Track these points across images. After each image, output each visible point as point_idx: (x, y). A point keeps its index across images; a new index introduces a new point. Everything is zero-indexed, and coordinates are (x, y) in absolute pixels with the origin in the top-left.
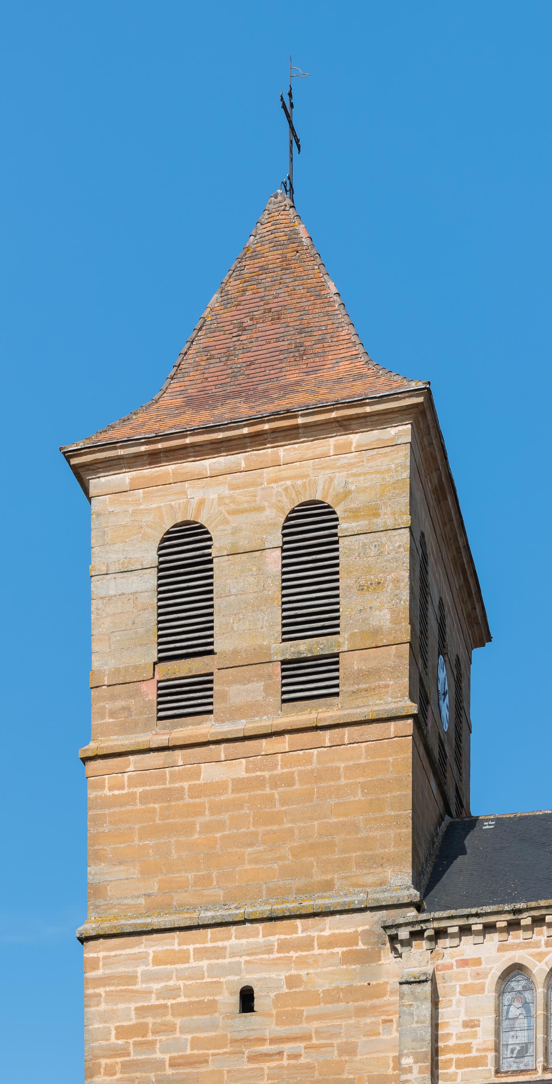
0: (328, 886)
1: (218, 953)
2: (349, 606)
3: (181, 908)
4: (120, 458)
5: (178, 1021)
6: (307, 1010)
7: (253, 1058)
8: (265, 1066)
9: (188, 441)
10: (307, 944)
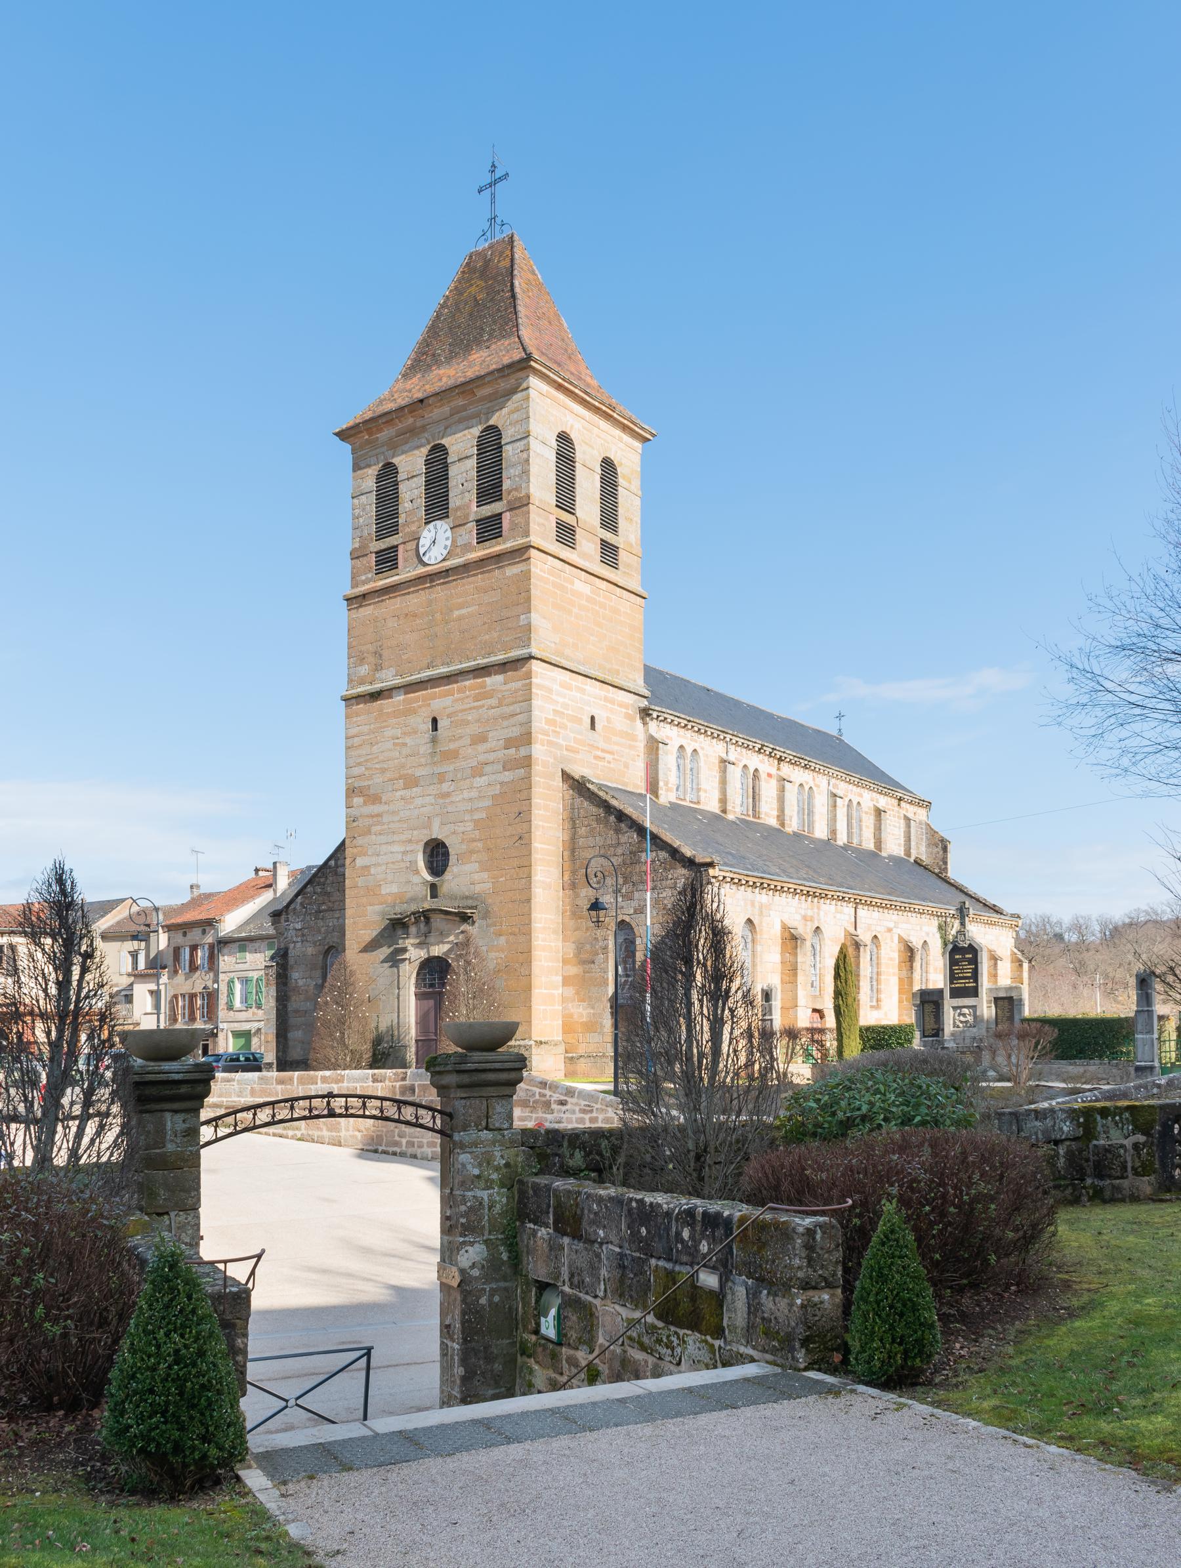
0: (618, 672)
1: (583, 691)
2: (622, 523)
3: (567, 658)
4: (548, 377)
5: (569, 724)
6: (614, 739)
7: (596, 757)
8: (601, 763)
9: (577, 391)
10: (612, 702)
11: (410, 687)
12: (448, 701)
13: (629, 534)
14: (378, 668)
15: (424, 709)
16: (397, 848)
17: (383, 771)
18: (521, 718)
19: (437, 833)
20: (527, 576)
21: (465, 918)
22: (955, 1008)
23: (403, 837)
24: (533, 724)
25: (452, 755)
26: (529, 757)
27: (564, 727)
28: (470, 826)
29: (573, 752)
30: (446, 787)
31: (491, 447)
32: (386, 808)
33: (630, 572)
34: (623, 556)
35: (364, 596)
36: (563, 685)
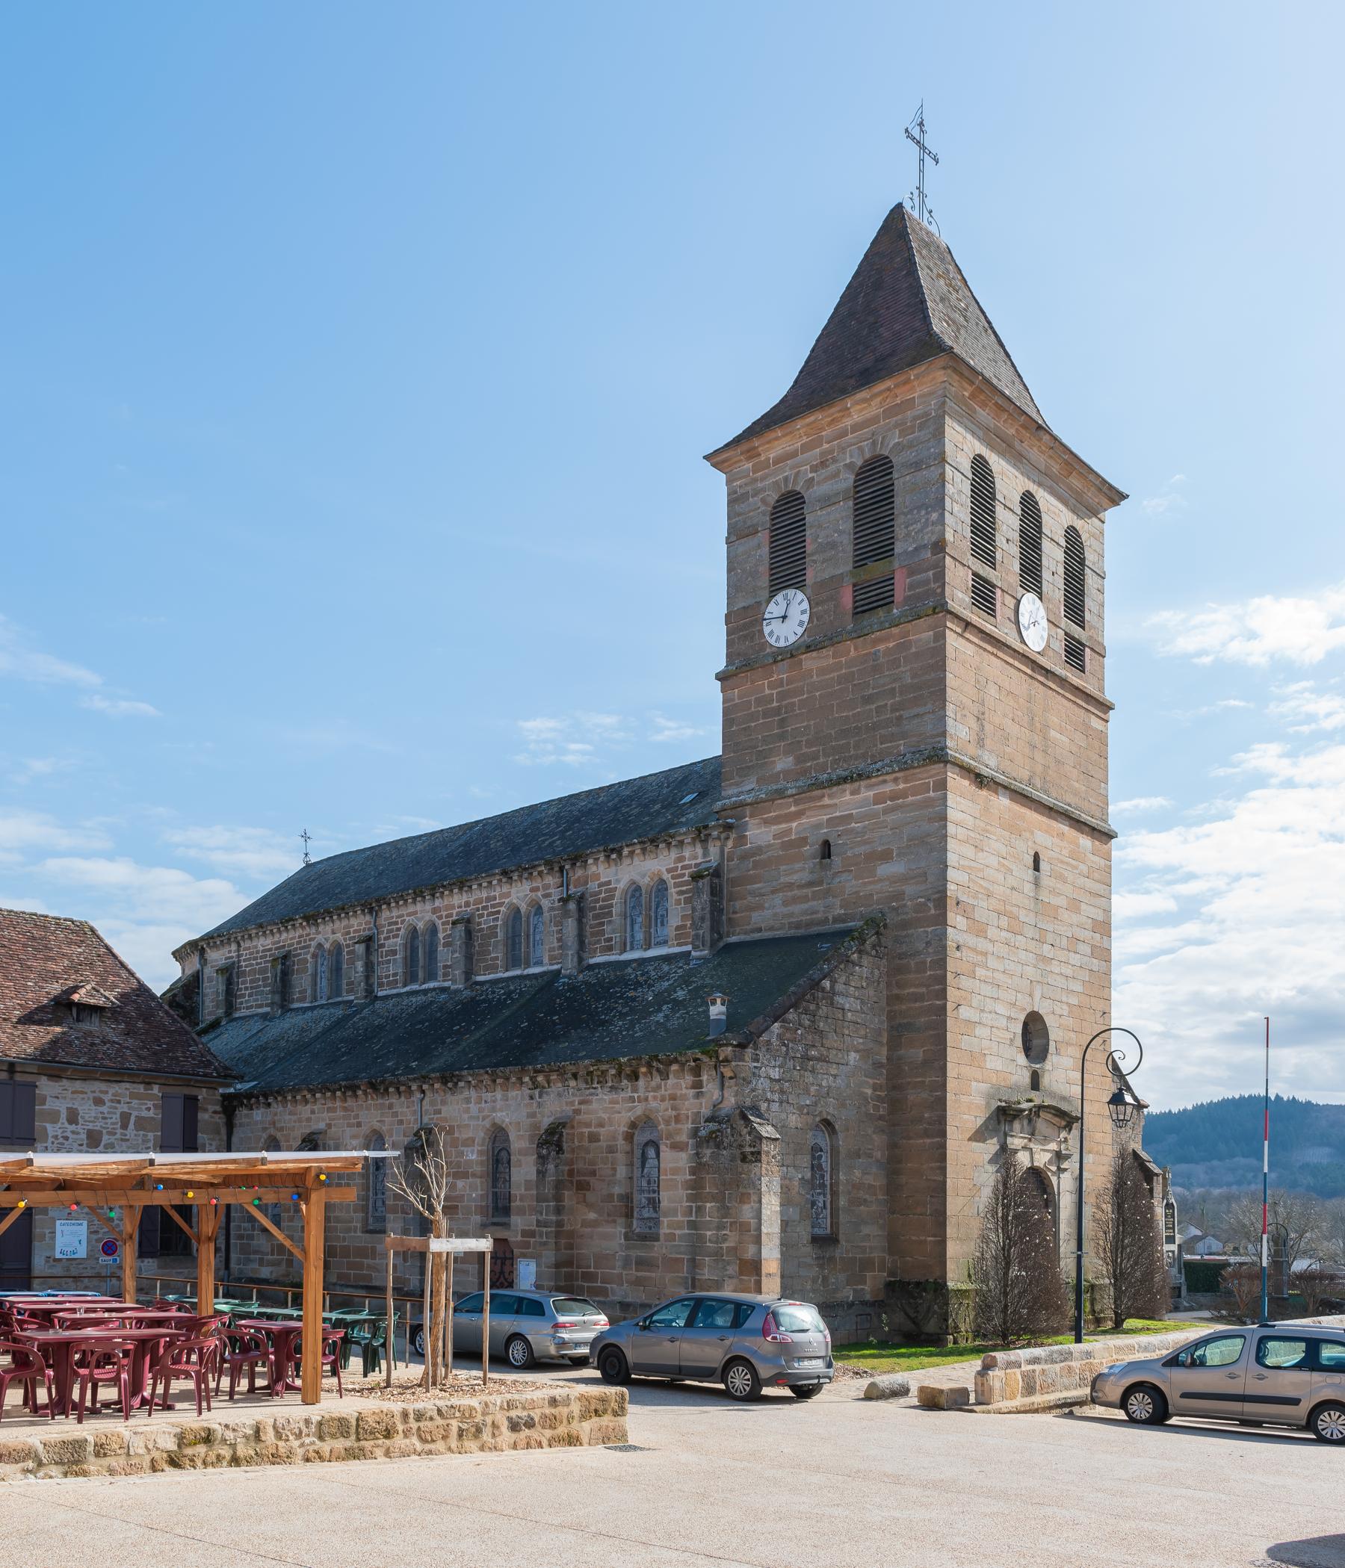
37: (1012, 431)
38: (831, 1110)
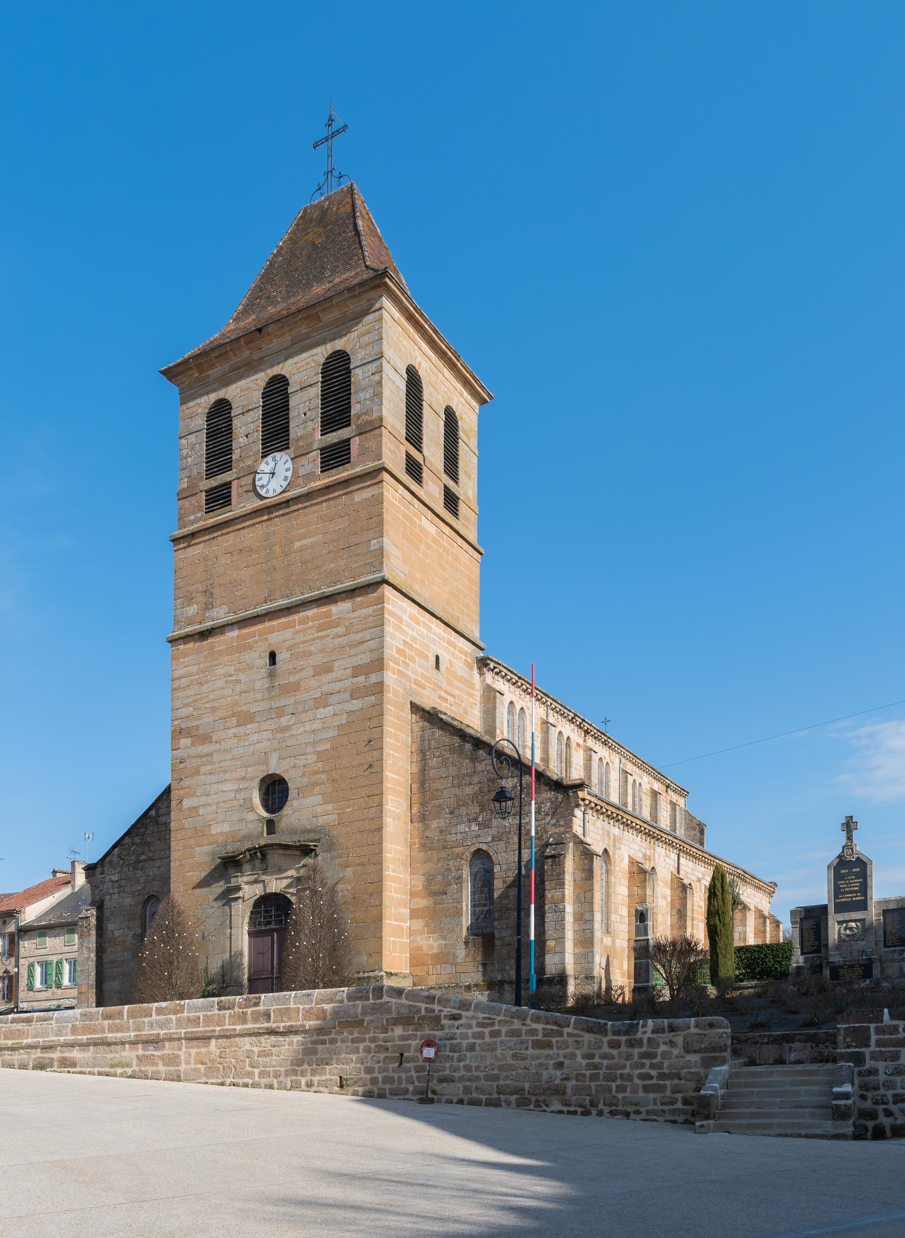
1: (429, 629)
6: (456, 683)
10: (454, 646)
11: (243, 623)
12: (288, 634)
13: (468, 488)
14: (209, 606)
15: (260, 644)
16: (228, 787)
17: (214, 710)
18: (372, 644)
19: (274, 767)
20: (379, 500)
21: (306, 851)
22: (840, 923)
23: (237, 775)
24: (386, 650)
25: (294, 688)
26: (382, 683)
27: (413, 661)
28: (312, 758)
29: (421, 687)
30: (284, 721)
31: (337, 376)
32: (217, 746)
33: (468, 519)
34: (462, 507)
35: (193, 535)
36: (412, 617)
37: (247, 353)
38: (156, 889)
